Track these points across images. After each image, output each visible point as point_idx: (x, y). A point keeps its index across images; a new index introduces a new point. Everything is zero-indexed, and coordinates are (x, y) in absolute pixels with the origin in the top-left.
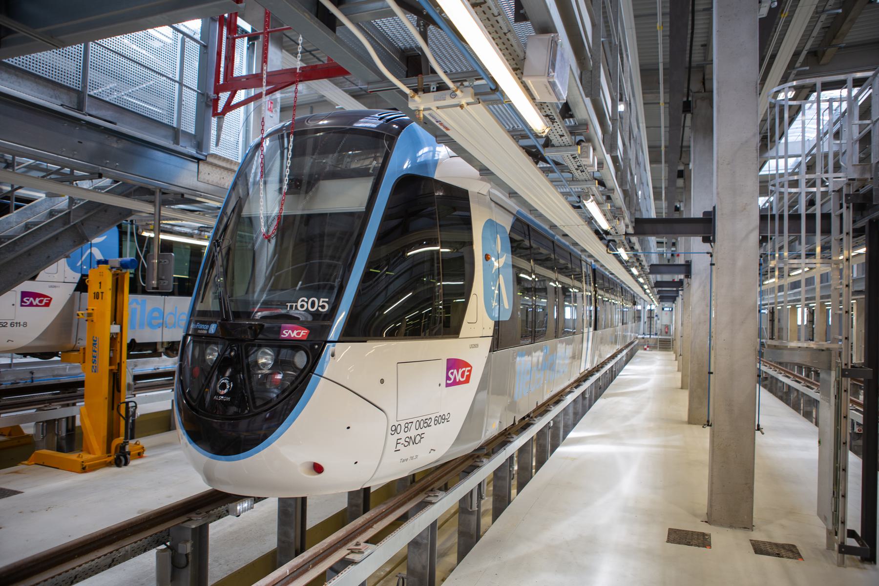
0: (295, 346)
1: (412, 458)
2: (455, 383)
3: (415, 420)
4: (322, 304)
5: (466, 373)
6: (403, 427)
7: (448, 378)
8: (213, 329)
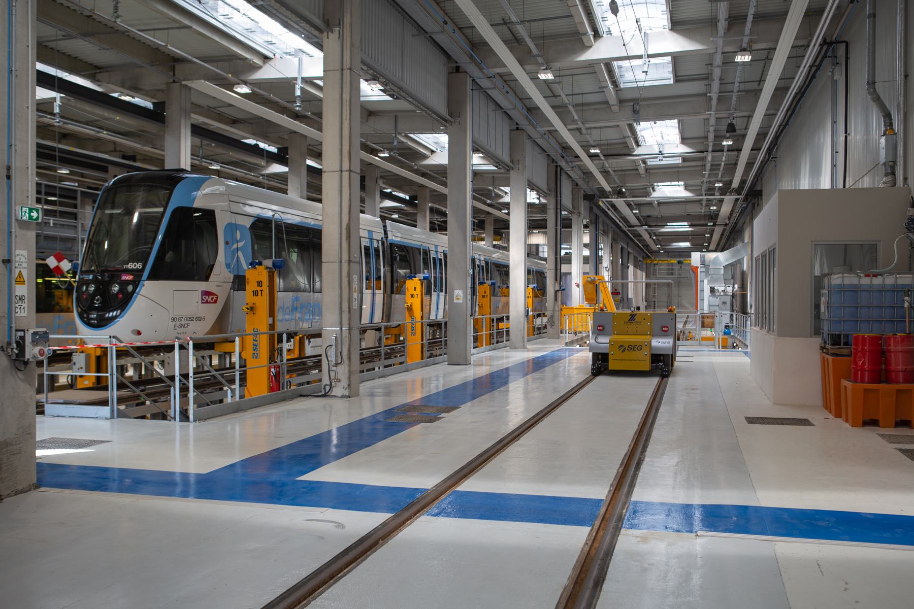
0: (128, 283)
2: (207, 302)
4: (139, 266)
8: (91, 277)
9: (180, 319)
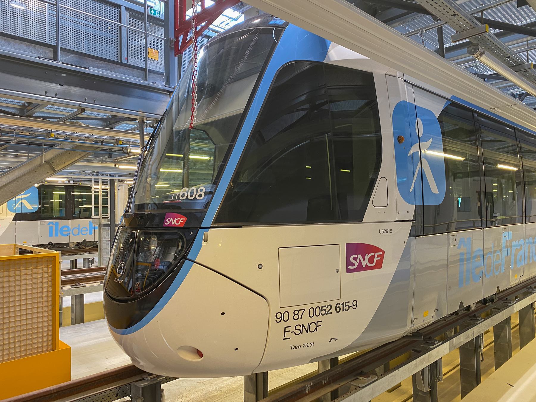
1: (306, 345)
2: (360, 268)
3: (307, 308)
5: (376, 259)
6: (292, 315)
7: (349, 263)
9: (297, 315)
